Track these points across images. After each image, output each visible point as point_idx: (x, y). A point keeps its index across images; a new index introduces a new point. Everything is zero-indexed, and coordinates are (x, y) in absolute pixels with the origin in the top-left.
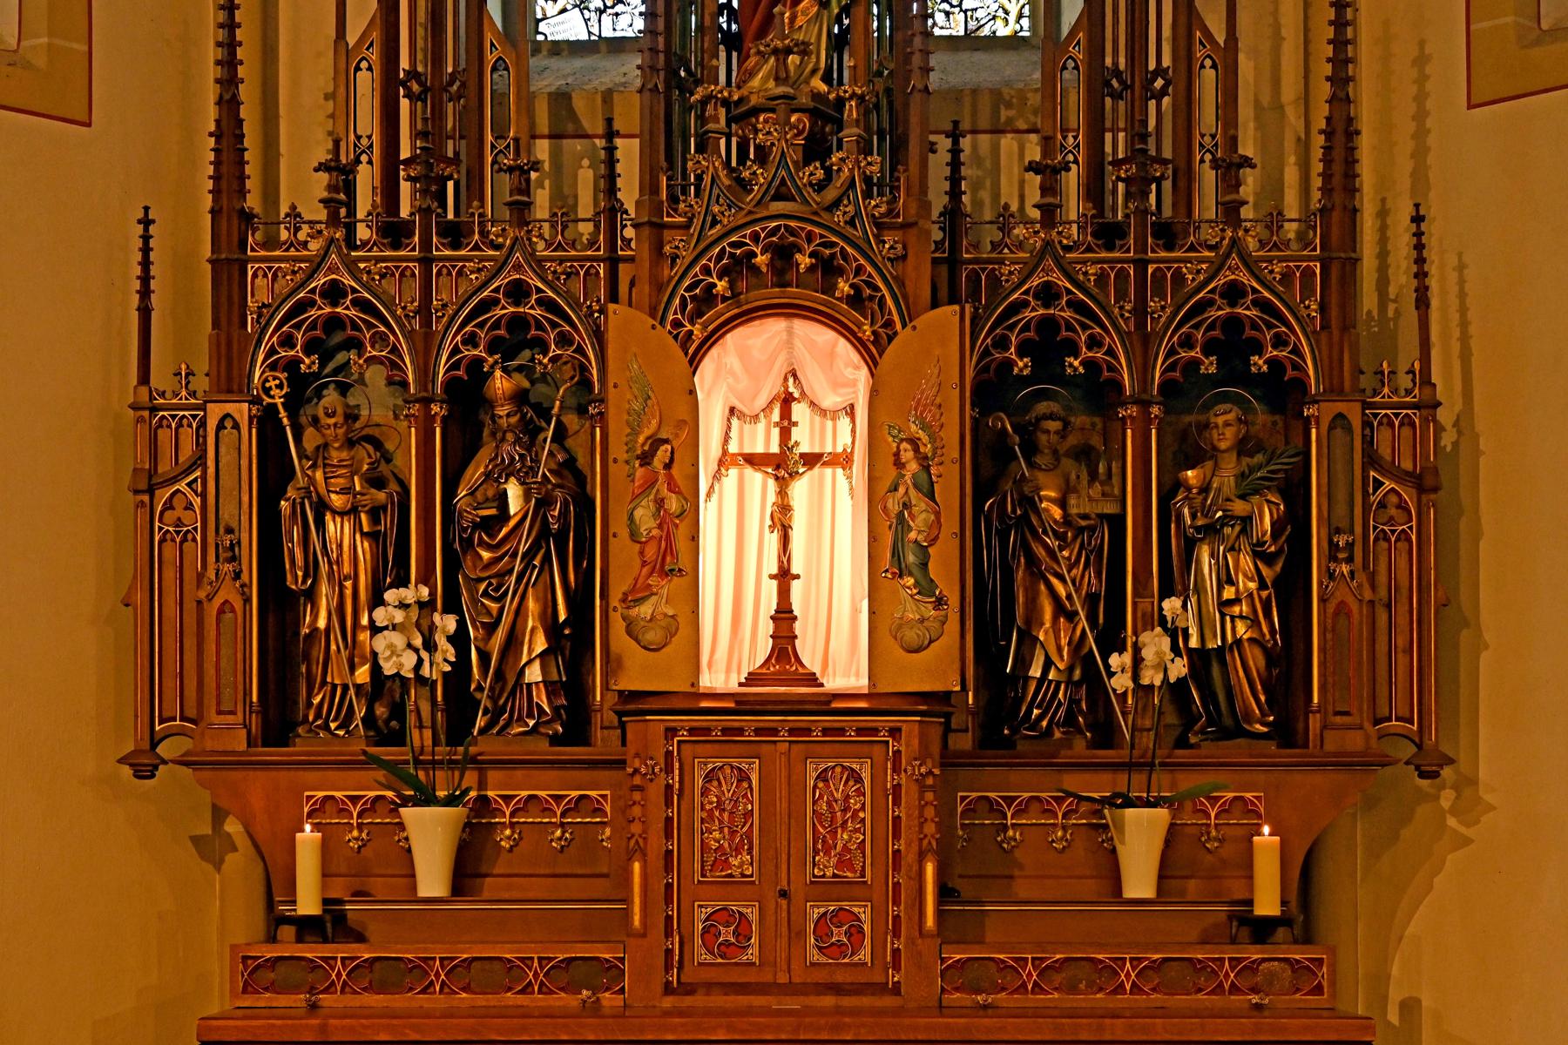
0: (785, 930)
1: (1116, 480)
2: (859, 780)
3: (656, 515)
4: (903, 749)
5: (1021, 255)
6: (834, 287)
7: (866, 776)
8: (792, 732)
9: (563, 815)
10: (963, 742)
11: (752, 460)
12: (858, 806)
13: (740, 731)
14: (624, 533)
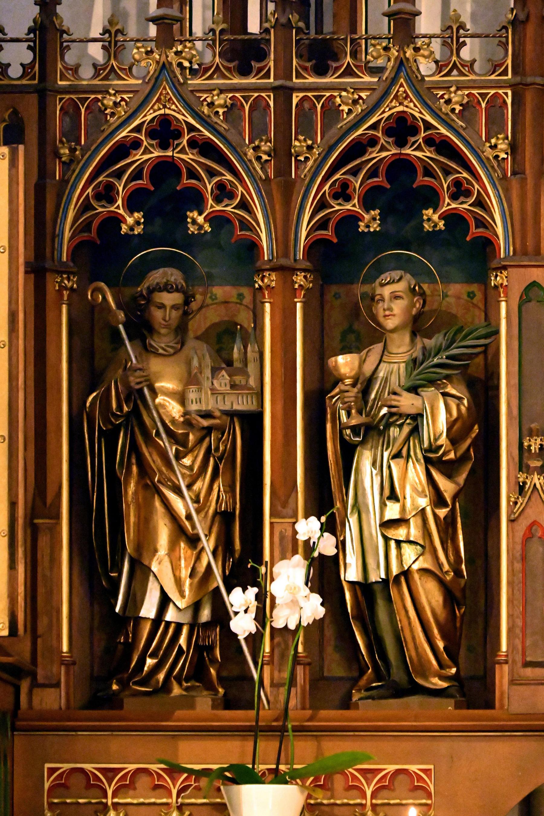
1: (252, 368)
5: (132, 81)
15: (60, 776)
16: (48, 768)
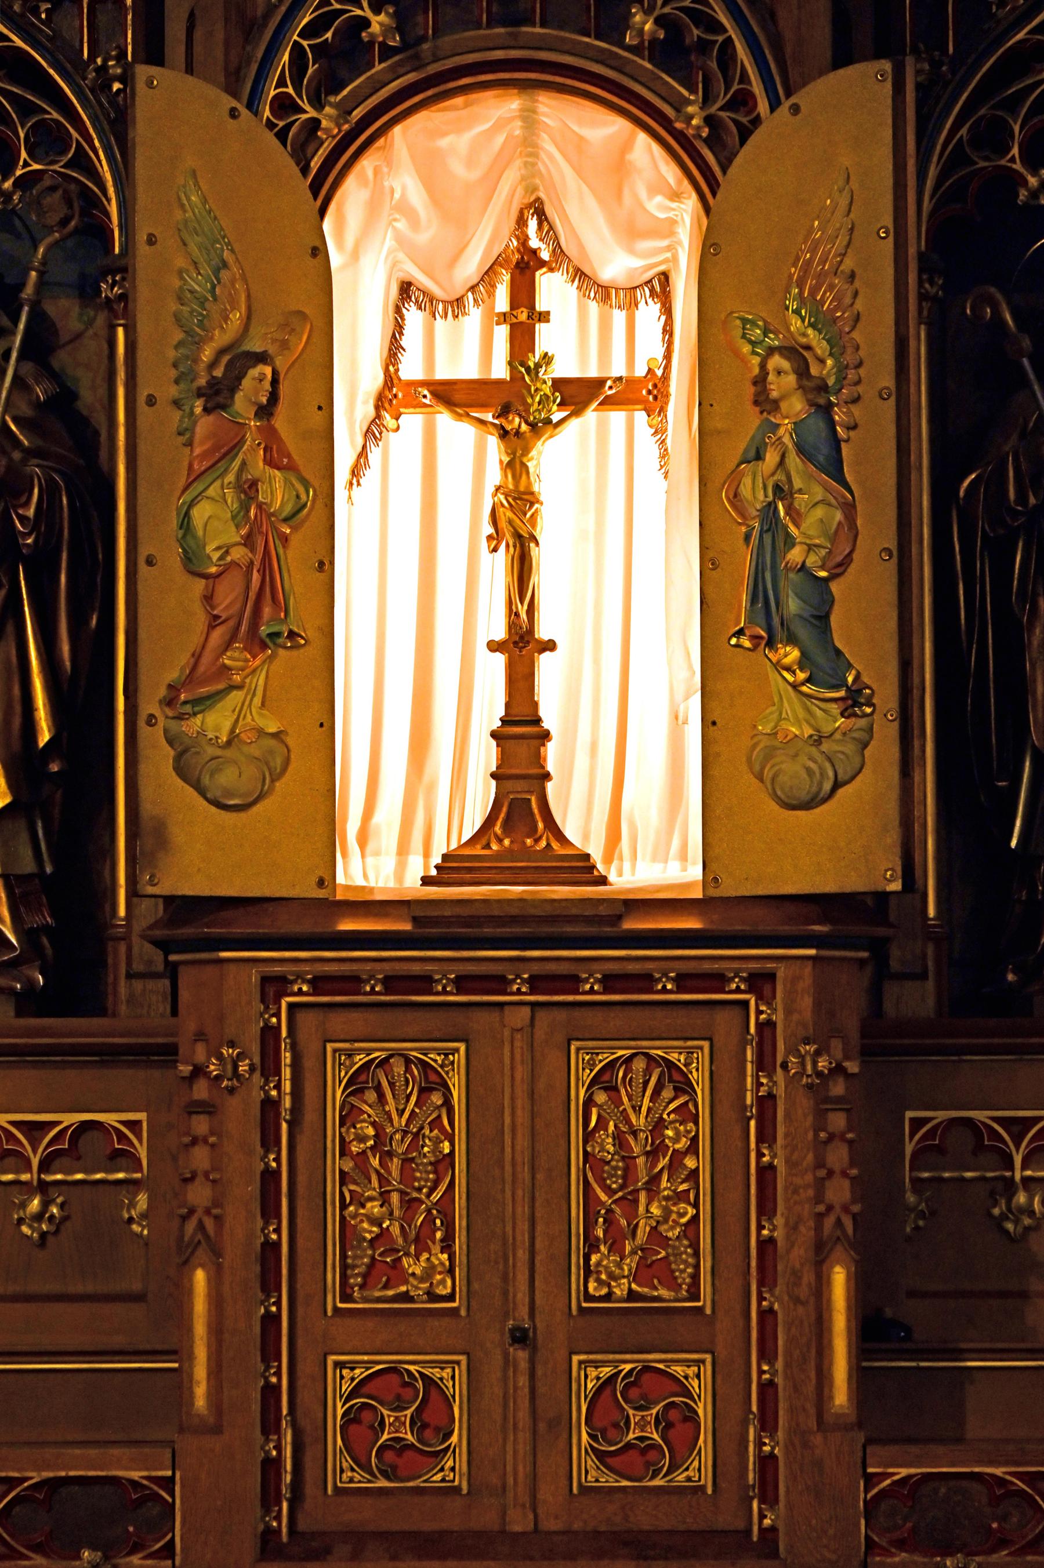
0: (524, 1415)
2: (684, 1087)
3: (239, 517)
4: (778, 1018)
6: (624, 22)
7: (699, 1077)
8: (536, 983)
9: (45, 1166)
10: (916, 1000)
11: (450, 395)
12: (682, 1144)
13: (424, 983)
14: (172, 558)
15: (931, 1134)
16: (911, 1119)
